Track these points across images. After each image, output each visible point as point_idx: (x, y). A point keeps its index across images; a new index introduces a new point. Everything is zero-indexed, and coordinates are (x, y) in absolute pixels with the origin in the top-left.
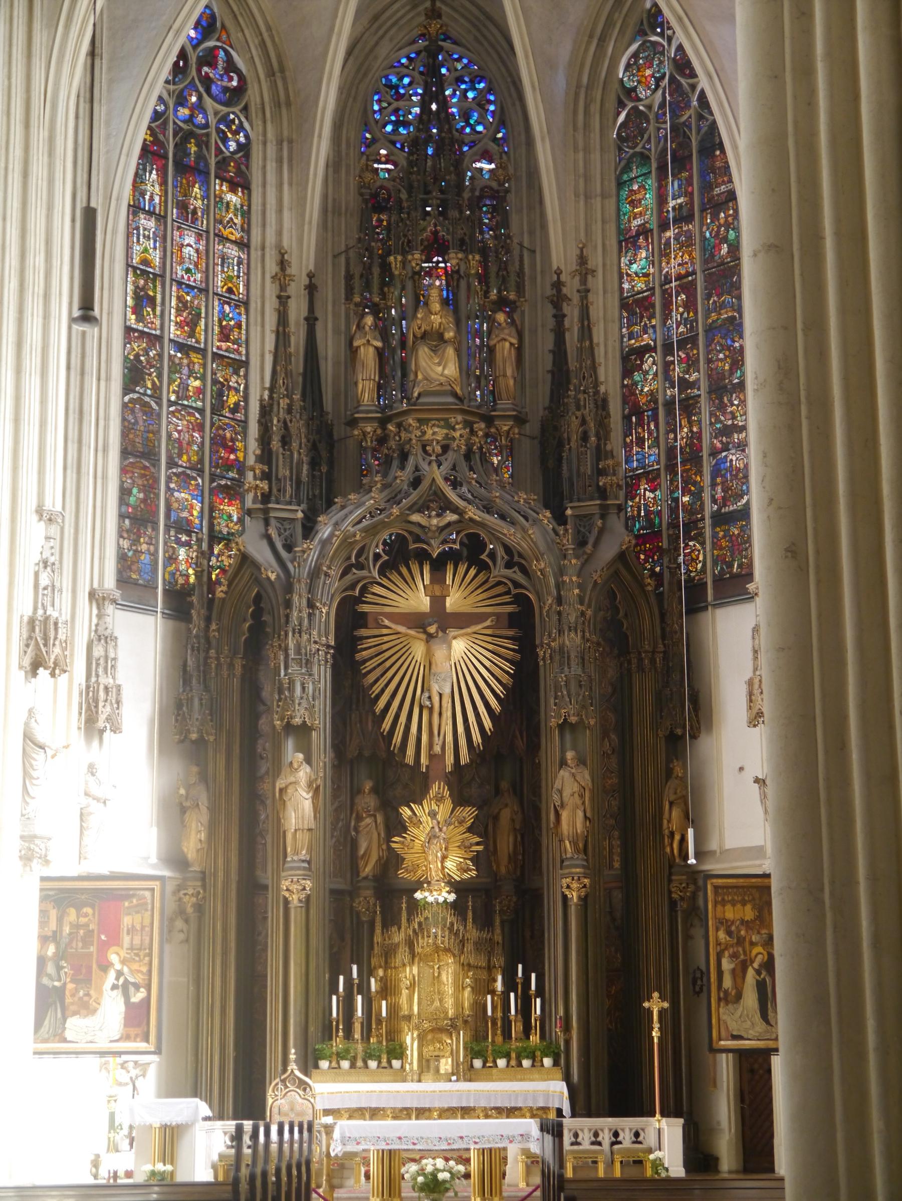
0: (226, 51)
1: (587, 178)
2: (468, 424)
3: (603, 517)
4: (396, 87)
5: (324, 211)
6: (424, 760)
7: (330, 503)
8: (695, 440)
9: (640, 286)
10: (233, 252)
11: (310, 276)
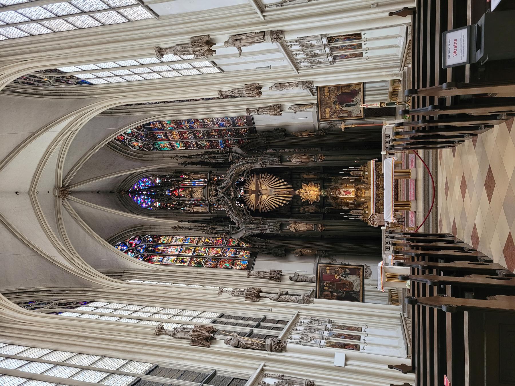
2: (211, 185)
3: (232, 152)
6: (291, 196)
8: (216, 131)
9: (182, 145)
10: (174, 239)
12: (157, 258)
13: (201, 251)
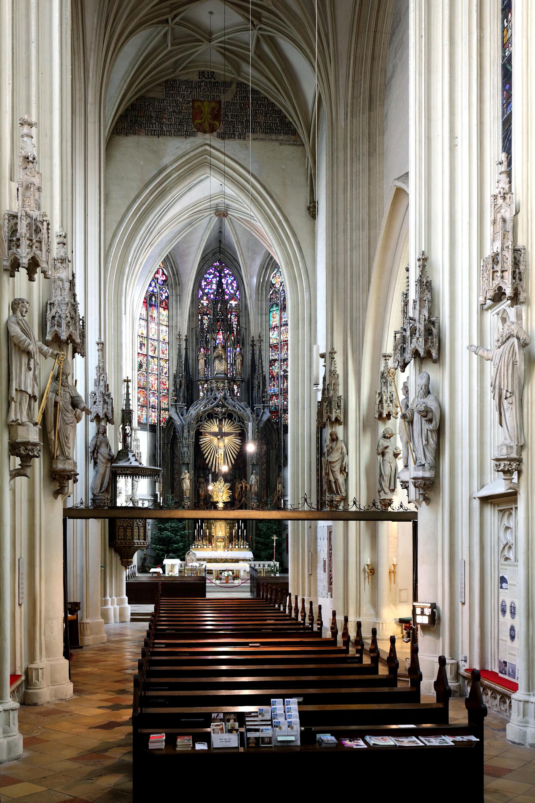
0: (162, 270)
1: (262, 309)
4: (209, 278)
5: (189, 316)
7: (192, 403)
9: (275, 342)
10: (165, 328)
11: (186, 336)
12: (144, 312)
13: (153, 365)
